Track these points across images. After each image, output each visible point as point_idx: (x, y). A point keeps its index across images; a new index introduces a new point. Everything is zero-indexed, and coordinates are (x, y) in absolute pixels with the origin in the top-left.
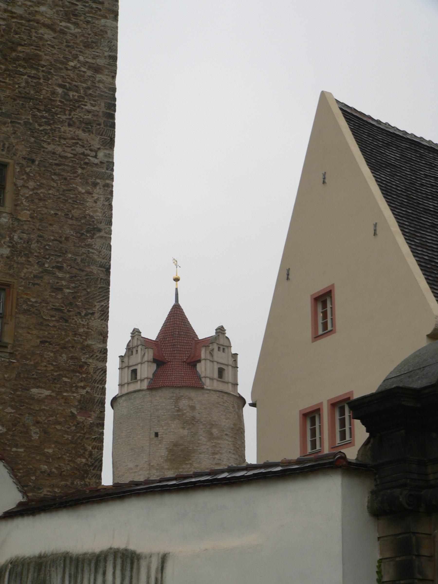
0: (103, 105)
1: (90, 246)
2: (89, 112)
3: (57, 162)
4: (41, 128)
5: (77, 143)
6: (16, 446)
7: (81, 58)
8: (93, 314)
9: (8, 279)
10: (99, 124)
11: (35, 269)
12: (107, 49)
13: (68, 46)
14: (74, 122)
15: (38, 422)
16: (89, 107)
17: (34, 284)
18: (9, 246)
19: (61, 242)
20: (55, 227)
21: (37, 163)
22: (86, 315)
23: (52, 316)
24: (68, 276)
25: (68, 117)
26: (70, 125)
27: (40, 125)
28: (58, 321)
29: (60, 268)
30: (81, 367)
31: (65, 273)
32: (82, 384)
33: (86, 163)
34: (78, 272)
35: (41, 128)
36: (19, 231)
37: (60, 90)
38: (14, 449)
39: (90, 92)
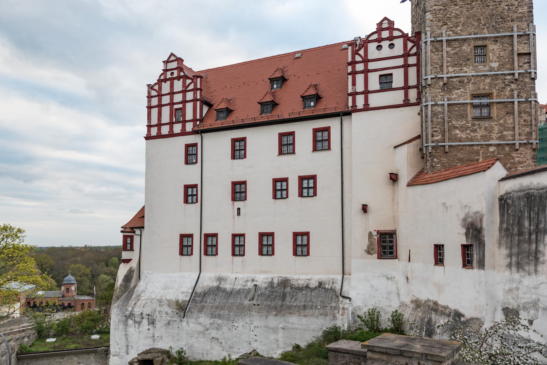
2: (520, 13)
4: (499, 26)
10: (526, 17)
14: (514, 19)
16: (520, 11)
27: (499, 25)
39: (521, 4)
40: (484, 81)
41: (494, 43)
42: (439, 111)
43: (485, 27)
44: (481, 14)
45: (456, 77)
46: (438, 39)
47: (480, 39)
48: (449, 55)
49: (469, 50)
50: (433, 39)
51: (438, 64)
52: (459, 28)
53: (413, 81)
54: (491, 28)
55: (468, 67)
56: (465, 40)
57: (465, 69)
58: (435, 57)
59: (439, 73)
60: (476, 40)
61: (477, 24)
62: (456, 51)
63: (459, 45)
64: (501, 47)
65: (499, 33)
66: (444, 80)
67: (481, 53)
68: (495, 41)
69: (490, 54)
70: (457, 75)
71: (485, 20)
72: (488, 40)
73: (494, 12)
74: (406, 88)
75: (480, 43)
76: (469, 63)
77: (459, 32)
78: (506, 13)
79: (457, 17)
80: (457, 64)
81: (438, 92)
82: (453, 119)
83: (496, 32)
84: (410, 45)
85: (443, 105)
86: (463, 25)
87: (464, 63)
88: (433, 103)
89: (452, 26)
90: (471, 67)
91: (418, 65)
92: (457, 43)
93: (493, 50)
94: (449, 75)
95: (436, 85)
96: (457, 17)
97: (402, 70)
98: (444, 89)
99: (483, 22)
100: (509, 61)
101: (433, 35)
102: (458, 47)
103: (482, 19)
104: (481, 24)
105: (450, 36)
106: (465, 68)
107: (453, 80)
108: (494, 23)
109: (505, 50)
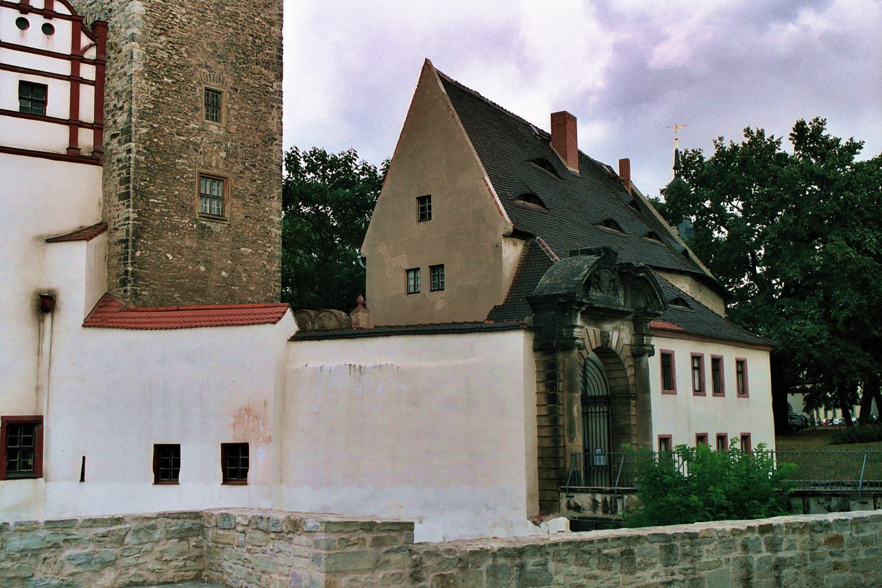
0: (275, 49)
1: (270, 150)
3: (250, 91)
4: (241, 66)
5: (261, 77)
6: (234, 286)
7: (262, 15)
8: (273, 197)
9: (225, 174)
11: (240, 167)
12: (277, 8)
13: (254, 6)
14: (259, 62)
15: (245, 270)
16: (267, 51)
17: (240, 177)
18: (225, 151)
19: (254, 148)
20: (250, 138)
21: (239, 91)
22: (270, 198)
23: (251, 199)
24: (258, 171)
25: (256, 58)
26: (257, 64)
27: (240, 64)
28: (254, 202)
29: (254, 166)
30: (268, 233)
31: (257, 169)
32: (269, 245)
33: (267, 92)
34: (265, 169)
35: (241, 66)
36: (230, 140)
37: (251, 39)
38: (233, 288)
39: (268, 40)
40: (218, 154)
53: (87, 113)
74: (74, 123)
82: (171, 210)
84: (85, 41)
91: (99, 84)
97: (67, 85)
100: (251, 128)
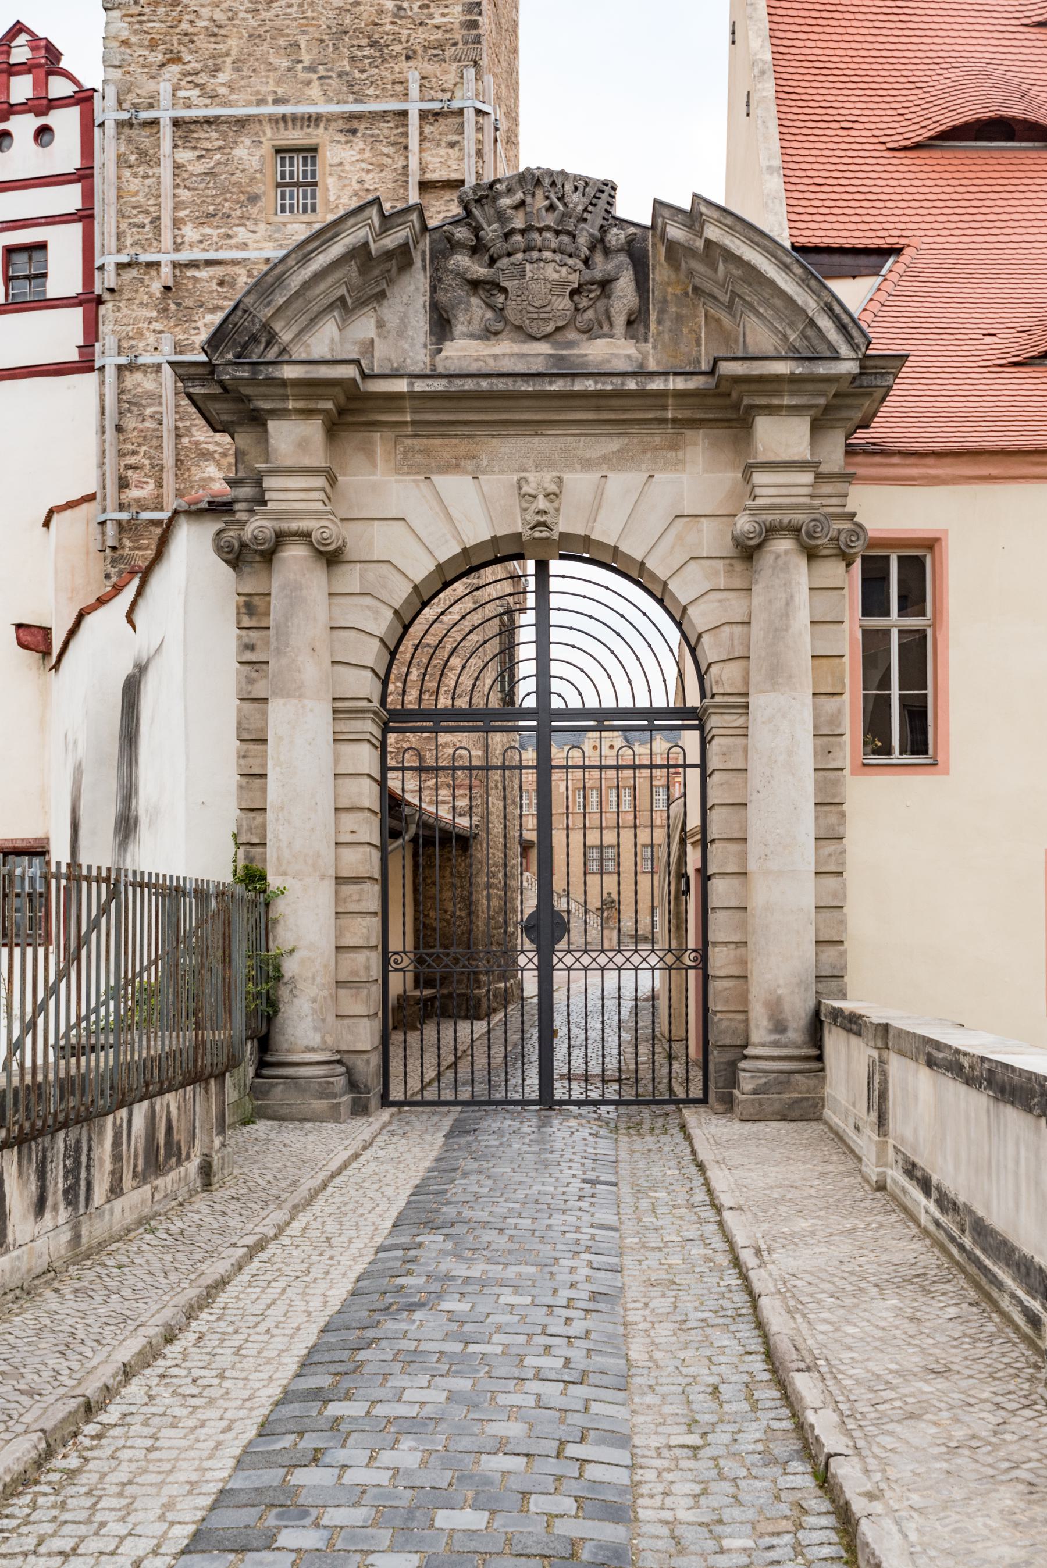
4: (364, 76)
27: (362, 71)
35: (364, 76)
41: (343, 139)
42: (146, 392)
43: (315, 77)
44: (301, 25)
45: (209, 263)
46: (144, 115)
47: (296, 120)
48: (184, 180)
49: (255, 163)
50: (125, 116)
51: (147, 212)
52: (223, 77)
54: (335, 83)
55: (253, 228)
56: (242, 123)
57: (241, 234)
58: (135, 184)
59: (150, 244)
60: (282, 125)
61: (286, 63)
62: (212, 164)
63: (221, 143)
64: (368, 154)
65: (361, 101)
66: (162, 275)
67: (305, 177)
68: (348, 131)
69: (331, 181)
70: (211, 255)
71: (315, 51)
72: (322, 125)
73: (348, 20)
75: (295, 137)
76: (254, 211)
77: (222, 90)
78: (389, 27)
79: (215, 35)
80: (214, 216)
81: (146, 319)
83: (351, 98)
85: (158, 367)
86: (238, 65)
87: (238, 213)
88: (123, 360)
89: (198, 66)
90: (262, 227)
92: (214, 135)
93: (341, 164)
94: (184, 256)
95: (137, 291)
96: (215, 35)
98: (166, 310)
99: (307, 59)
101: (131, 98)
102: (220, 148)
103: (303, 45)
104: (300, 66)
105: (189, 107)
106: (242, 229)
107: (197, 273)
108: (346, 62)
109: (382, 167)
